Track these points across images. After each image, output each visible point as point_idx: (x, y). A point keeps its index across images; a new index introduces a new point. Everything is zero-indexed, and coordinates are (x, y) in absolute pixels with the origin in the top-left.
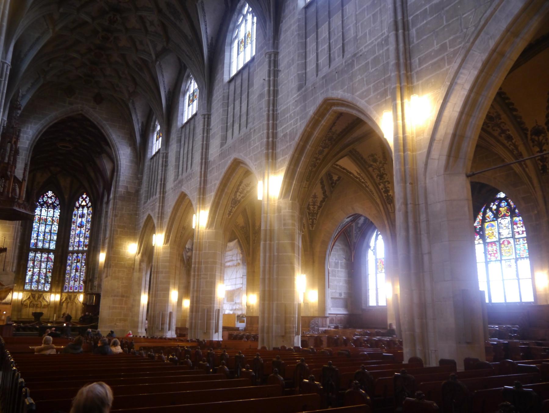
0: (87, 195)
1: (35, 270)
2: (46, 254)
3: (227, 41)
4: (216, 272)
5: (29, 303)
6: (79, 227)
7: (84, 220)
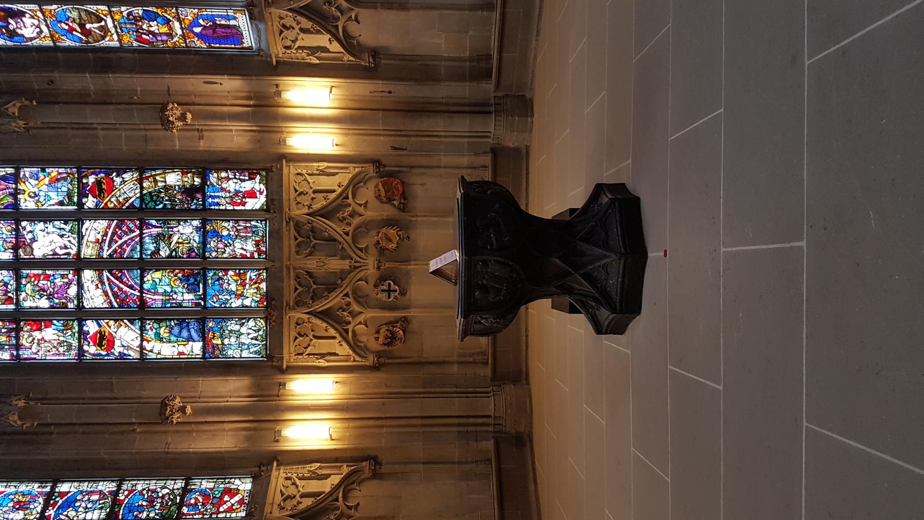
1: (95, 298)
5: (370, 314)
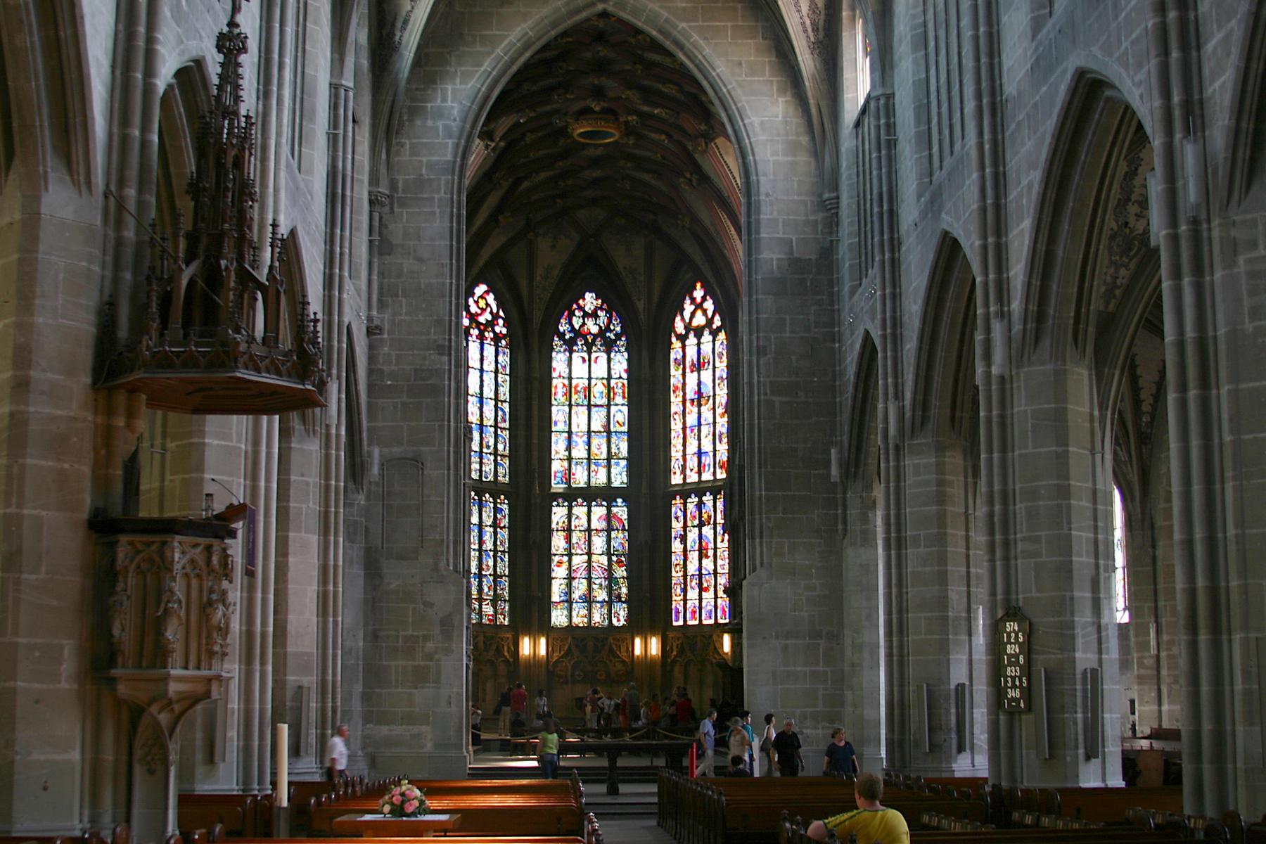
0: (708, 292)
2: (602, 506)
4: (1070, 529)
6: (692, 401)
7: (706, 375)
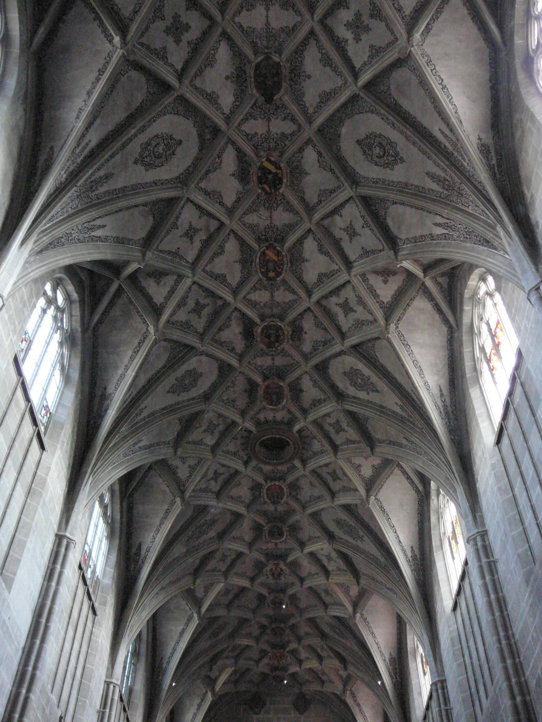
3: (434, 544)
